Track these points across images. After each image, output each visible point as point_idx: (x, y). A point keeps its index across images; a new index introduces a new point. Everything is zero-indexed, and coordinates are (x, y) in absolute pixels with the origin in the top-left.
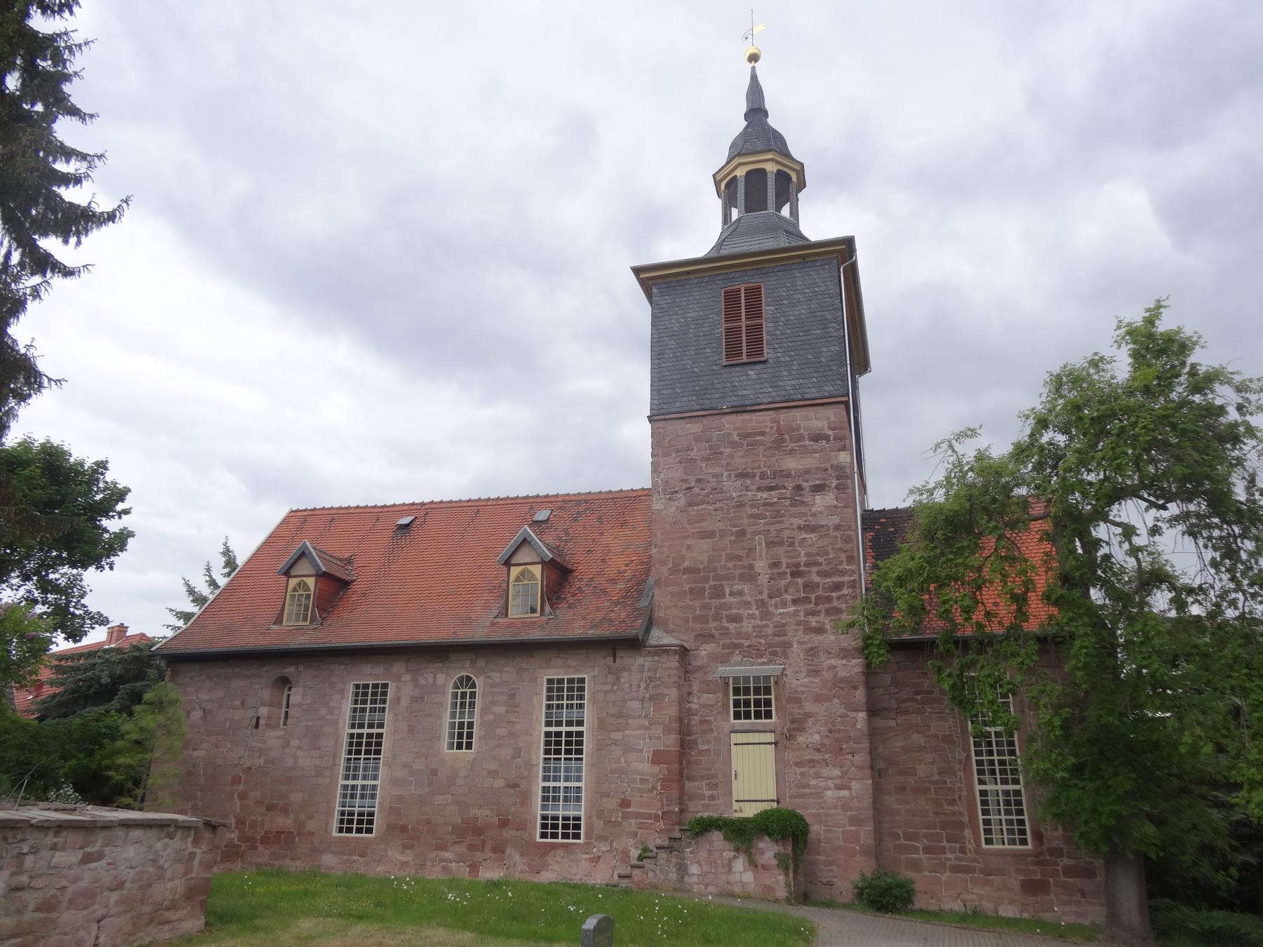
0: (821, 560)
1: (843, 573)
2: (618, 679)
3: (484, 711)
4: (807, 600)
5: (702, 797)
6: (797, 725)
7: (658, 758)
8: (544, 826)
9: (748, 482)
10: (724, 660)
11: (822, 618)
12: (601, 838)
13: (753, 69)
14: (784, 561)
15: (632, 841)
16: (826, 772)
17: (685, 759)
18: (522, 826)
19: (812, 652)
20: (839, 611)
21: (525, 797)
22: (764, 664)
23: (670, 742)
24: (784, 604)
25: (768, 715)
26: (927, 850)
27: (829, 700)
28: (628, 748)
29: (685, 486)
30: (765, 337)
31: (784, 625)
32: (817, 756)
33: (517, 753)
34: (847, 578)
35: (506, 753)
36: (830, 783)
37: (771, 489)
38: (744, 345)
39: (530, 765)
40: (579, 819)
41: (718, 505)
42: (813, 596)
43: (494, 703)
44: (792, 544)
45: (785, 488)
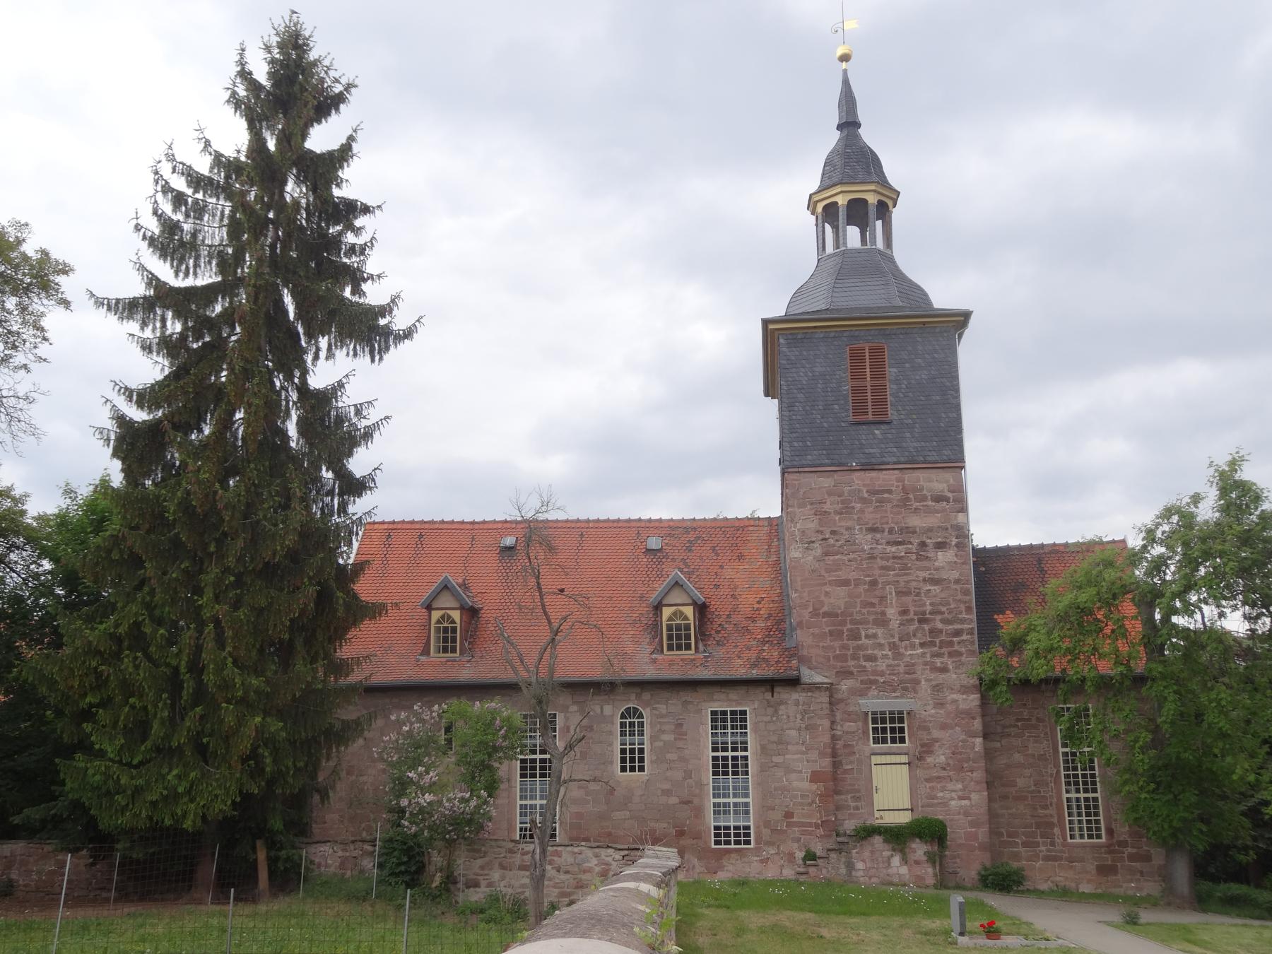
0: (943, 609)
1: (962, 621)
2: (776, 711)
3: (654, 739)
4: (932, 644)
5: (848, 807)
6: (927, 748)
7: (815, 777)
8: (716, 835)
9: (878, 536)
10: (863, 693)
11: (945, 659)
12: (769, 844)
13: (845, 71)
14: (912, 609)
15: (796, 845)
16: (950, 786)
17: (838, 781)
18: (698, 836)
19: (937, 688)
20: (960, 654)
21: (699, 812)
22: (896, 697)
23: (825, 764)
24: (913, 647)
25: (902, 740)
26: (1025, 844)
27: (952, 728)
28: (789, 770)
29: (821, 537)
30: (889, 398)
31: (913, 665)
32: (943, 774)
33: (688, 774)
34: (966, 626)
35: (678, 775)
36: (954, 795)
37: (899, 543)
38: (869, 408)
39: (701, 785)
40: (748, 828)
41: (852, 556)
42: (938, 641)
43: (663, 732)
44: (918, 594)
45: (911, 543)
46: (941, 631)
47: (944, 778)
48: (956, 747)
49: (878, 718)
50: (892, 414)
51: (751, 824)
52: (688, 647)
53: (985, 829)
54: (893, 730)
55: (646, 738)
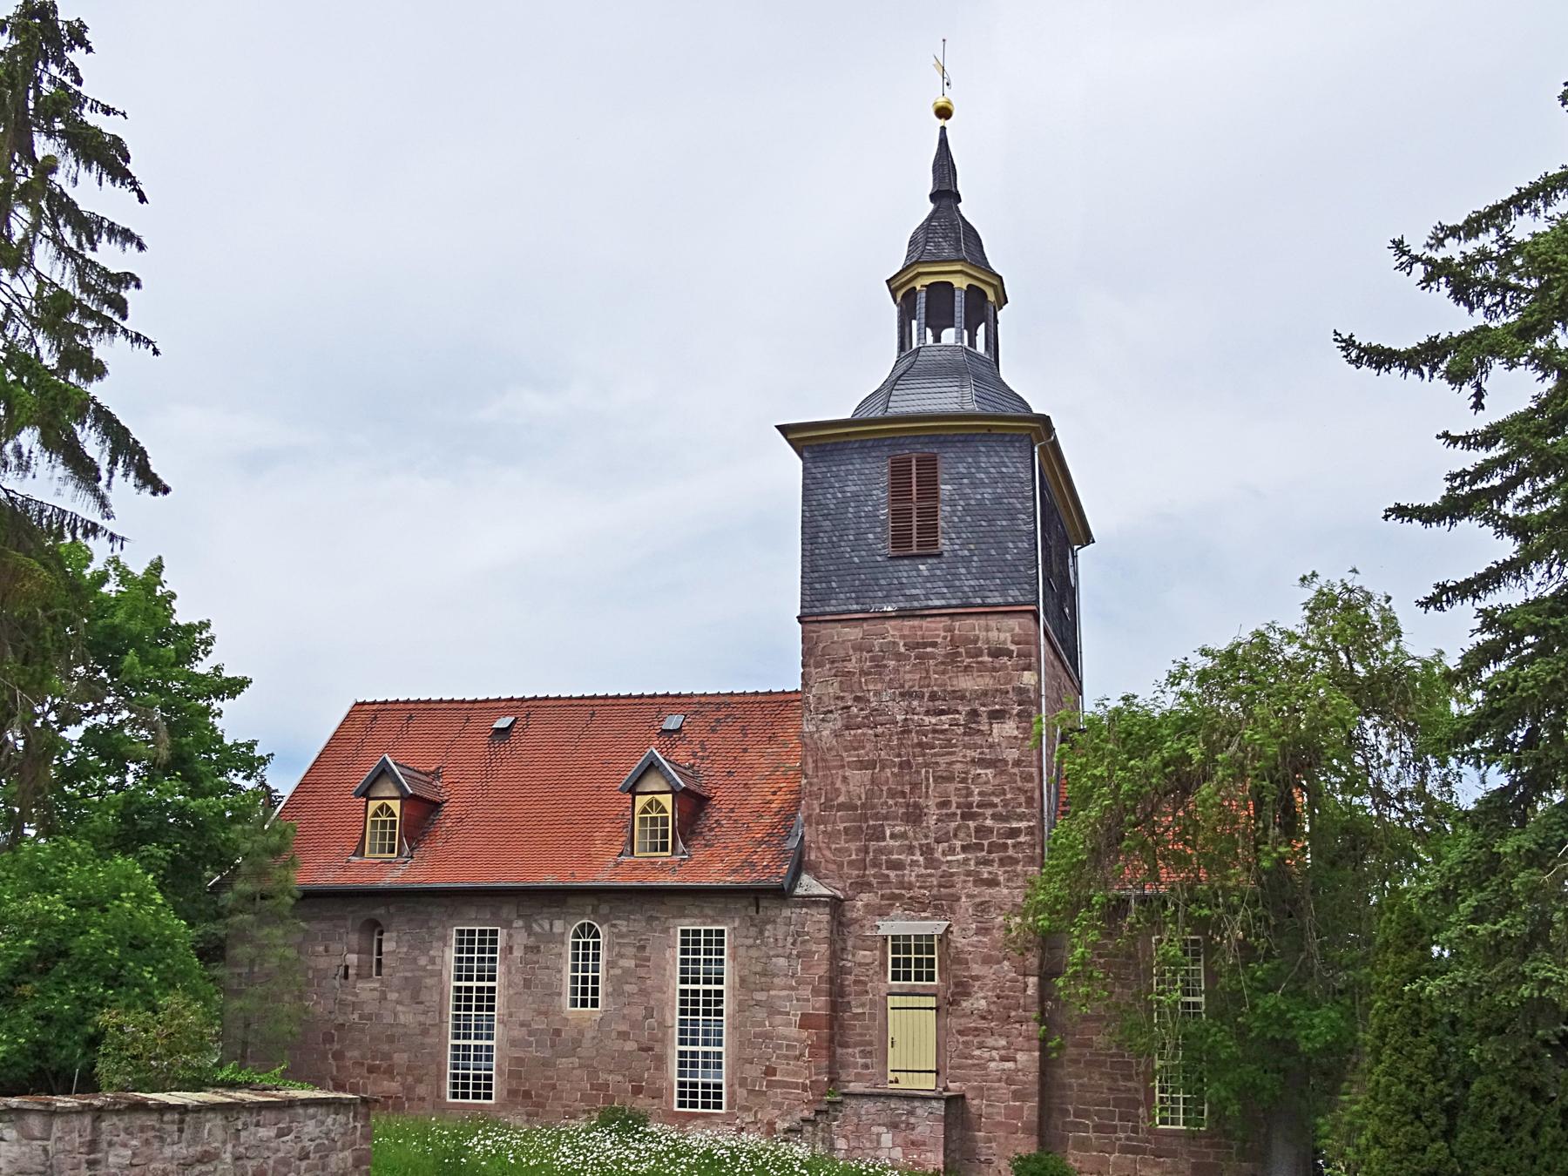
0: (996, 800)
1: (1021, 817)
2: (761, 932)
3: (611, 964)
4: (980, 847)
5: (855, 1065)
6: (963, 989)
7: (806, 1022)
8: (682, 1094)
9: (915, 703)
10: (882, 913)
11: (995, 868)
12: (747, 1109)
13: (943, 129)
14: (954, 799)
15: (777, 1112)
16: (990, 1042)
17: (838, 1027)
18: (657, 1094)
19: (982, 907)
20: (1016, 861)
21: (660, 1061)
22: (926, 919)
23: (819, 1006)
24: (952, 851)
25: (931, 977)
26: (1097, 1128)
27: (999, 962)
28: (773, 1011)
29: (841, 704)
30: (942, 524)
31: (952, 875)
32: (983, 1024)
33: (650, 1013)
34: (1023, 825)
35: (639, 1012)
36: (994, 1053)
37: (942, 713)
38: (914, 534)
39: (663, 1025)
40: (719, 1086)
41: (880, 730)
42: (986, 843)
43: (621, 956)
44: (964, 781)
45: (958, 712)
46: (991, 830)
47: (982, 1030)
48: (1002, 989)
49: (900, 944)
50: (944, 544)
51: (723, 1081)
52: (664, 847)
53: (1033, 1103)
54: (919, 962)
55: (602, 963)
